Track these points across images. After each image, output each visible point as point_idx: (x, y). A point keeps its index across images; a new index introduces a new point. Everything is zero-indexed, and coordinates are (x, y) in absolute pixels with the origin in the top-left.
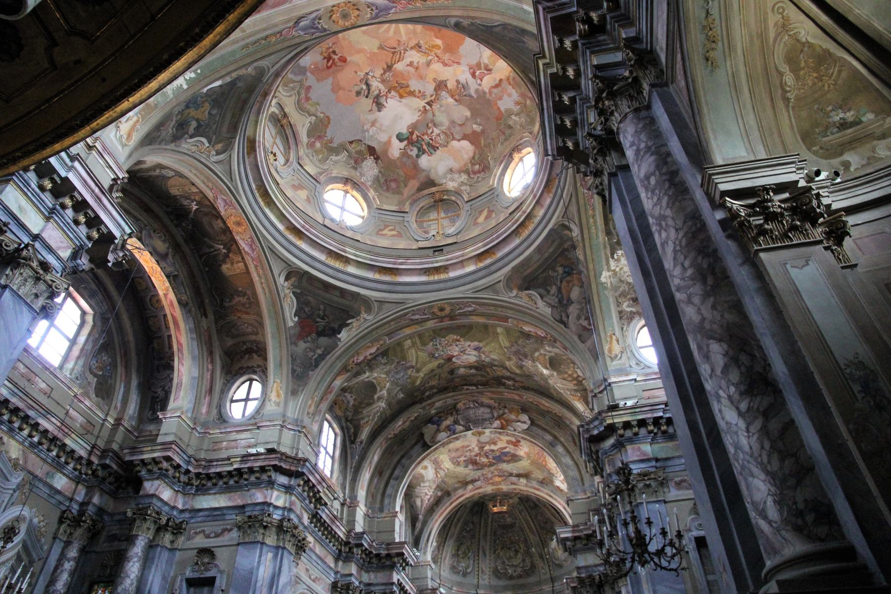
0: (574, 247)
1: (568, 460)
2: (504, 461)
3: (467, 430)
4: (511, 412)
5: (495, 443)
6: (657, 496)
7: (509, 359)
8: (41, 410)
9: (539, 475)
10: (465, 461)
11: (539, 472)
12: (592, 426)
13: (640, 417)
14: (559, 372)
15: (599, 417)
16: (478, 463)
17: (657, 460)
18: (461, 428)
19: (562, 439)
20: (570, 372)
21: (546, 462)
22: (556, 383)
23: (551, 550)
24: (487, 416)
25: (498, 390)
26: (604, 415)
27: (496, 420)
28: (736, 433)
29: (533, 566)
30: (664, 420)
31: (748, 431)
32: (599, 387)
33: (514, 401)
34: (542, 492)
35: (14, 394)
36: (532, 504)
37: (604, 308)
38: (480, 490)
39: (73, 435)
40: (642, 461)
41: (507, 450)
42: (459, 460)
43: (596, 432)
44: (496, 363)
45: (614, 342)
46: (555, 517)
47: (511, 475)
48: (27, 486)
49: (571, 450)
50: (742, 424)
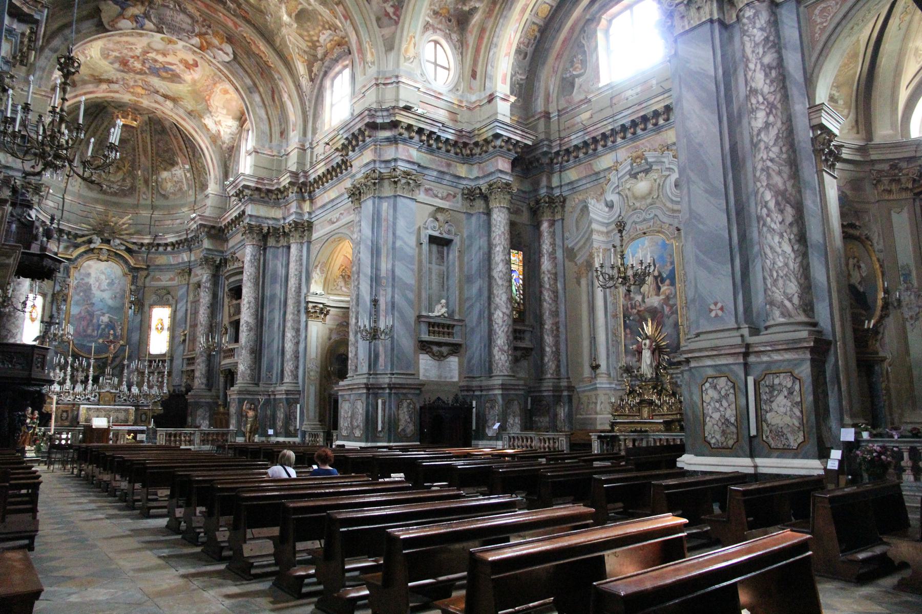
1: (262, 113)
2: (159, 76)
3: (158, 32)
4: (216, 34)
5: (164, 55)
6: (412, 194)
9: (190, 105)
10: (116, 57)
11: (193, 102)
12: (379, 114)
13: (422, 126)
14: (300, 26)
15: (391, 111)
16: (128, 66)
17: (419, 166)
18: (151, 26)
19: (261, 89)
20: (312, 33)
21: (210, 97)
22: (288, 35)
23: (160, 179)
24: (184, 26)
25: (216, 6)
26: (397, 111)
27: (196, 35)
28: (788, 258)
29: (133, 189)
30: (435, 136)
31: (795, 260)
32: (386, 79)
33: (225, 26)
34: (188, 123)
36: (159, 128)
37: (416, 7)
38: (116, 95)
40: (409, 162)
41: (173, 67)
42: (111, 53)
43: (379, 121)
45: (412, 45)
46: (181, 150)
47: (157, 92)
49: (266, 103)
50: (793, 255)
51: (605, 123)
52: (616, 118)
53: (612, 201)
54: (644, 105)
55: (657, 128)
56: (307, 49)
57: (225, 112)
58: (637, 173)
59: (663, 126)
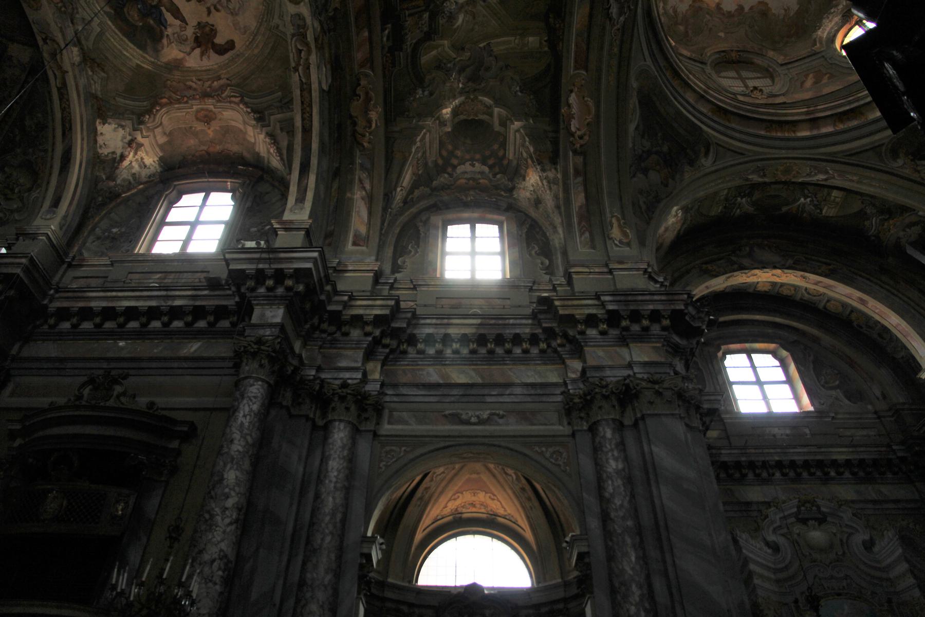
0: (691, 163)
7: (459, 48)
20: (459, 153)
21: (171, 103)
34: (80, 106)
44: (442, 21)
51: (772, 451)
52: (788, 451)
53: (774, 542)
54: (823, 450)
55: (826, 479)
56: (430, 164)
57: (162, 140)
58: (807, 520)
59: (833, 479)
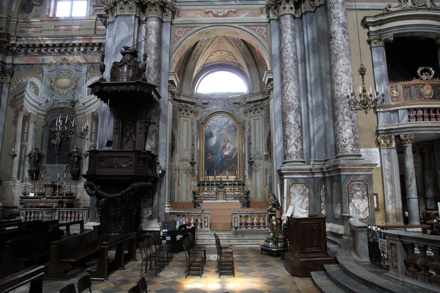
8: (69, 38)
35: (54, 40)
39: (93, 37)
48: (92, 69)
